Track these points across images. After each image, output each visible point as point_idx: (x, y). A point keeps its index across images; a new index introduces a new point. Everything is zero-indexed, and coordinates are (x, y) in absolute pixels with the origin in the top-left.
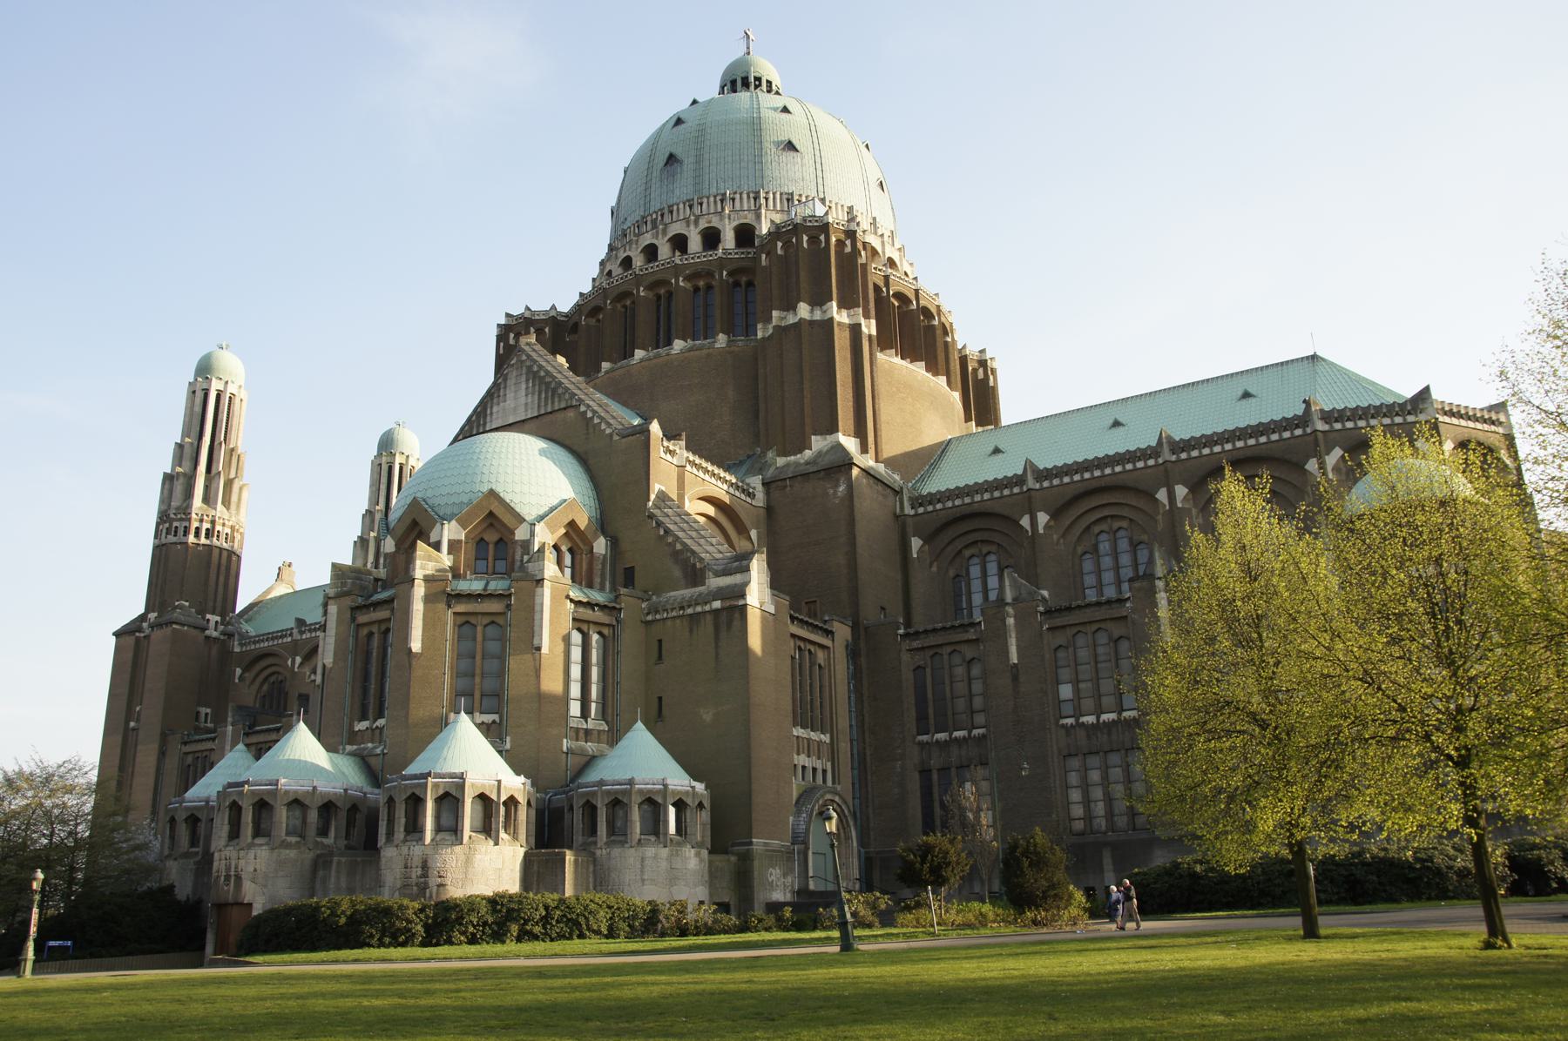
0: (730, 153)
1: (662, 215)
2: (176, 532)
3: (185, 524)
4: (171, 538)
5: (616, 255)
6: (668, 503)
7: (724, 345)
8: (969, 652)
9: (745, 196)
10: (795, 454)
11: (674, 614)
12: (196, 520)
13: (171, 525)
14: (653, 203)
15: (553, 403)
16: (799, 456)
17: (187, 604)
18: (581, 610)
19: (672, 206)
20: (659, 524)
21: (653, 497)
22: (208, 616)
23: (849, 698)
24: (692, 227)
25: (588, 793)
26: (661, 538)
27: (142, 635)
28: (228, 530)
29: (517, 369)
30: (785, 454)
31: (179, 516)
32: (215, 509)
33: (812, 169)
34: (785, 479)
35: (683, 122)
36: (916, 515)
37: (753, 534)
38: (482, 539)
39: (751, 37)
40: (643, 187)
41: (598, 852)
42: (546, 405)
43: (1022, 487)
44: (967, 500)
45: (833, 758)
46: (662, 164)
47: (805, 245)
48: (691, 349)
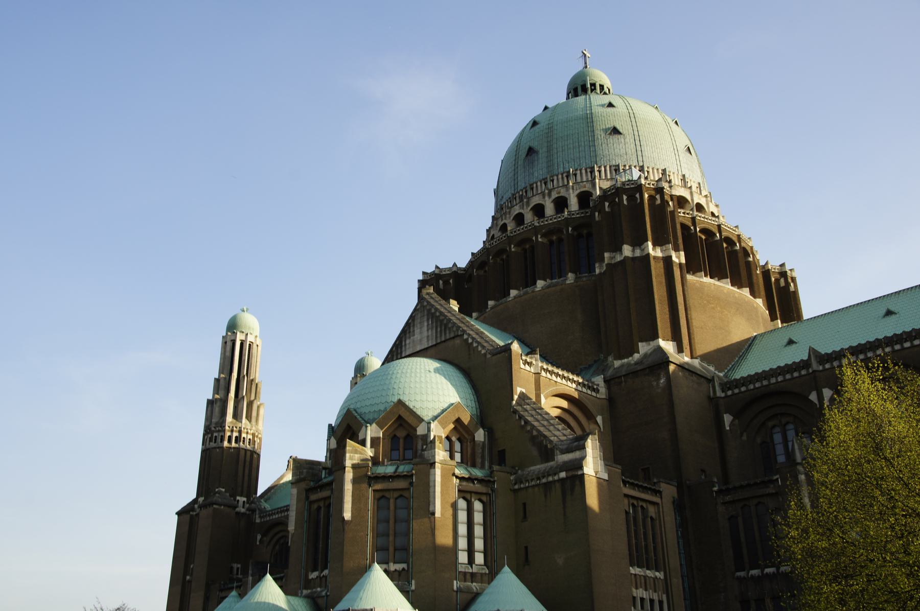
0: (571, 142)
1: (526, 192)
2: (215, 440)
3: (221, 434)
4: (213, 445)
5: (497, 223)
6: (527, 401)
7: (572, 281)
9: (584, 171)
10: (628, 357)
11: (533, 483)
12: (228, 431)
13: (212, 435)
14: (519, 184)
15: (445, 334)
16: (630, 358)
17: (223, 490)
18: (464, 483)
19: (533, 184)
20: (521, 417)
21: (516, 397)
22: (238, 498)
23: (678, 542)
24: (547, 198)
26: (523, 427)
27: (195, 513)
28: (250, 437)
29: (421, 312)
30: (621, 358)
31: (217, 429)
32: (241, 423)
33: (633, 146)
34: (620, 377)
36: (726, 396)
37: (599, 419)
38: (395, 436)
39: (588, 55)
40: (512, 174)
42: (441, 336)
43: (808, 369)
44: (765, 383)
45: (667, 590)
46: (524, 155)
47: (625, 202)
48: (548, 287)
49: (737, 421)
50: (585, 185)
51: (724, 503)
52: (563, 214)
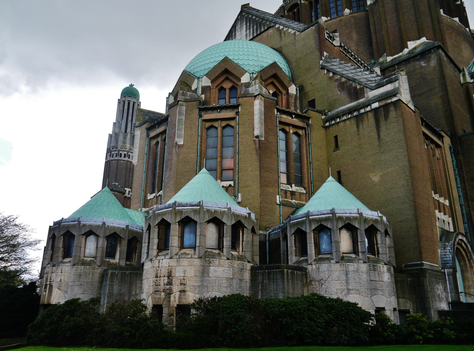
17: (117, 184)
25: (298, 223)
26: (331, 78)
31: (114, 149)
41: (309, 267)
45: (453, 215)
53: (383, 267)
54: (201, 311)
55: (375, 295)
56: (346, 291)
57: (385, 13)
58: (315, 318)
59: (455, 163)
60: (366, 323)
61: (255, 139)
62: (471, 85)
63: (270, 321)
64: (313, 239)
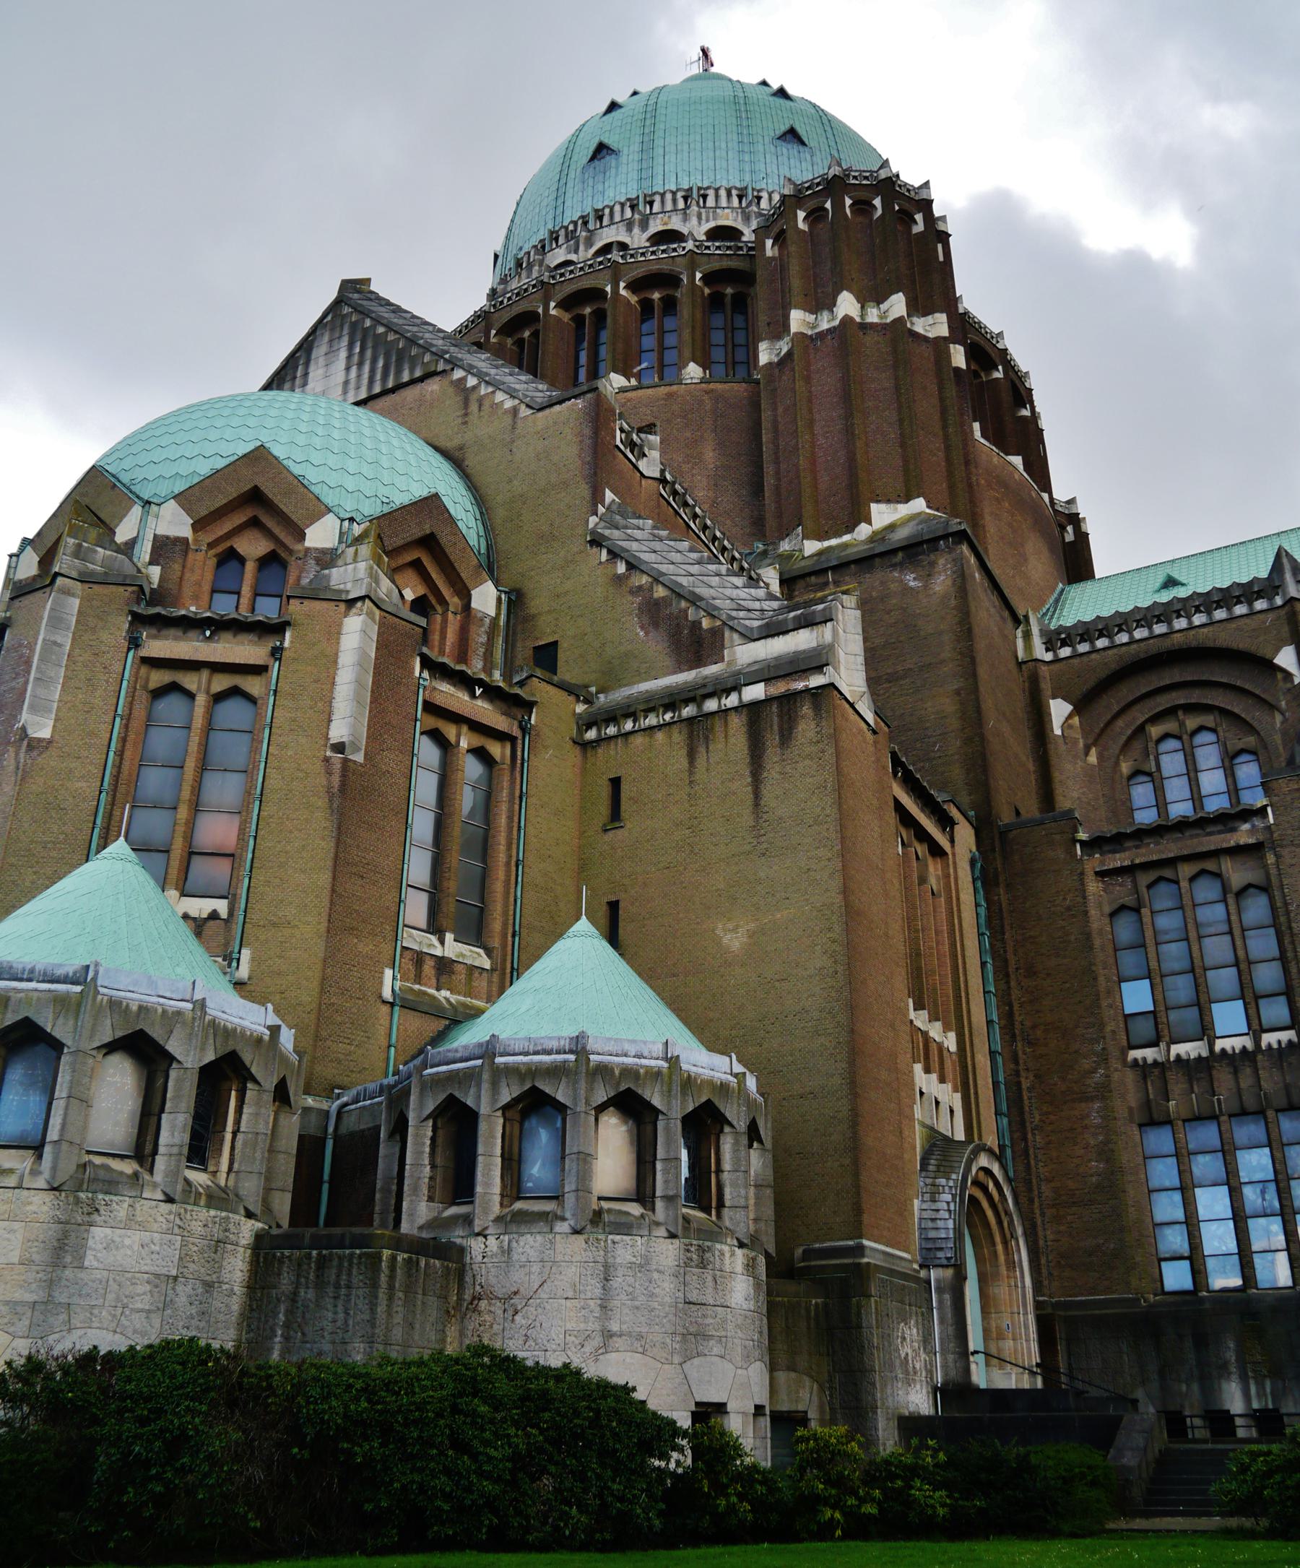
8: (1238, 874)
20: (614, 555)
24: (636, 230)
25: (451, 1076)
26: (619, 580)
34: (824, 571)
35: (620, 107)
36: (1057, 660)
41: (476, 1246)
43: (1271, 599)
44: (1159, 629)
49: (1076, 719)
50: (728, 214)
51: (1101, 874)
52: (683, 245)
53: (733, 1254)
54: (26, 1409)
55: (698, 1355)
56: (597, 1341)
57: (810, 401)
58: (475, 1443)
59: (982, 911)
60: (657, 1463)
61: (329, 753)
62: (1044, 670)
63: (306, 1454)
64: (499, 1141)
